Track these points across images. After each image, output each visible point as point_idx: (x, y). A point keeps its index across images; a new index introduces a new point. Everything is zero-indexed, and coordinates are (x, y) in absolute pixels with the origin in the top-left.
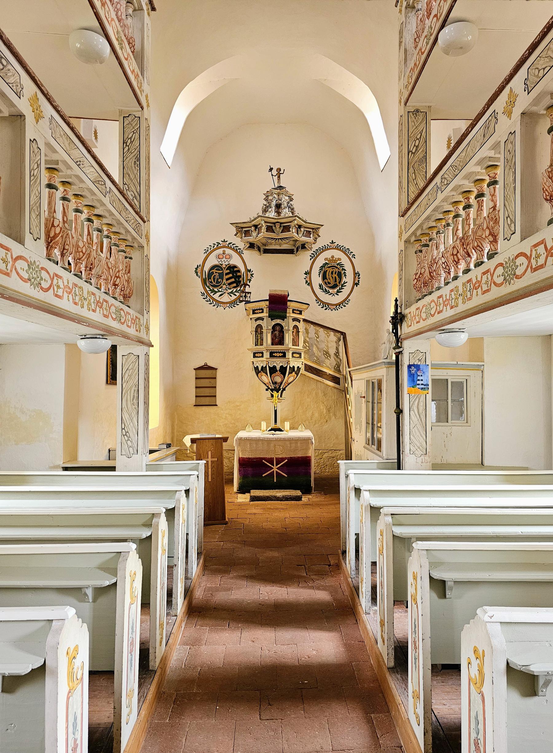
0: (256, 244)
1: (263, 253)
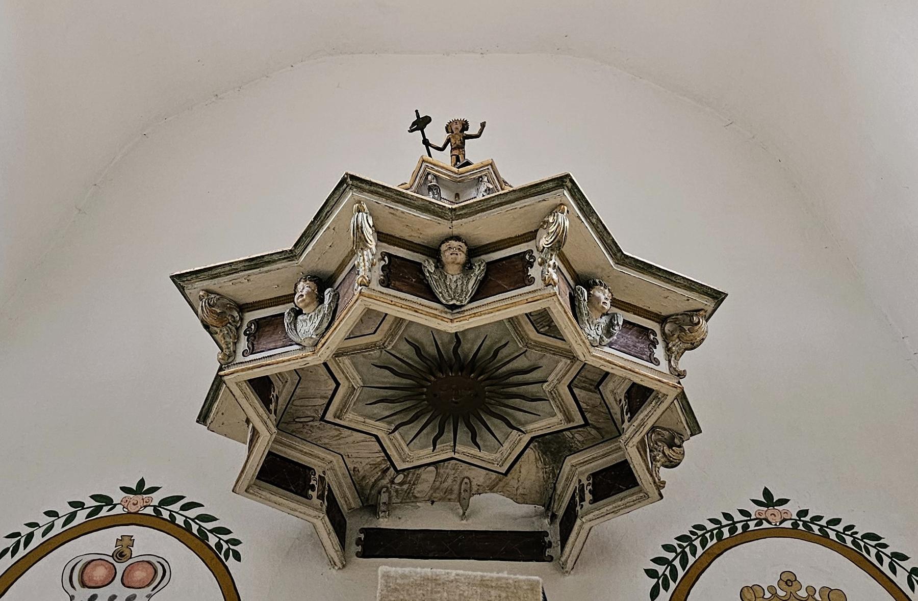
0: (319, 472)
1: (364, 555)
